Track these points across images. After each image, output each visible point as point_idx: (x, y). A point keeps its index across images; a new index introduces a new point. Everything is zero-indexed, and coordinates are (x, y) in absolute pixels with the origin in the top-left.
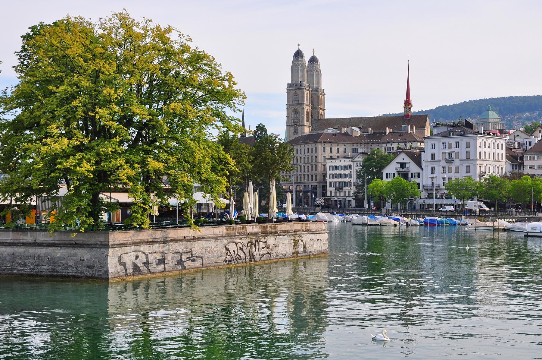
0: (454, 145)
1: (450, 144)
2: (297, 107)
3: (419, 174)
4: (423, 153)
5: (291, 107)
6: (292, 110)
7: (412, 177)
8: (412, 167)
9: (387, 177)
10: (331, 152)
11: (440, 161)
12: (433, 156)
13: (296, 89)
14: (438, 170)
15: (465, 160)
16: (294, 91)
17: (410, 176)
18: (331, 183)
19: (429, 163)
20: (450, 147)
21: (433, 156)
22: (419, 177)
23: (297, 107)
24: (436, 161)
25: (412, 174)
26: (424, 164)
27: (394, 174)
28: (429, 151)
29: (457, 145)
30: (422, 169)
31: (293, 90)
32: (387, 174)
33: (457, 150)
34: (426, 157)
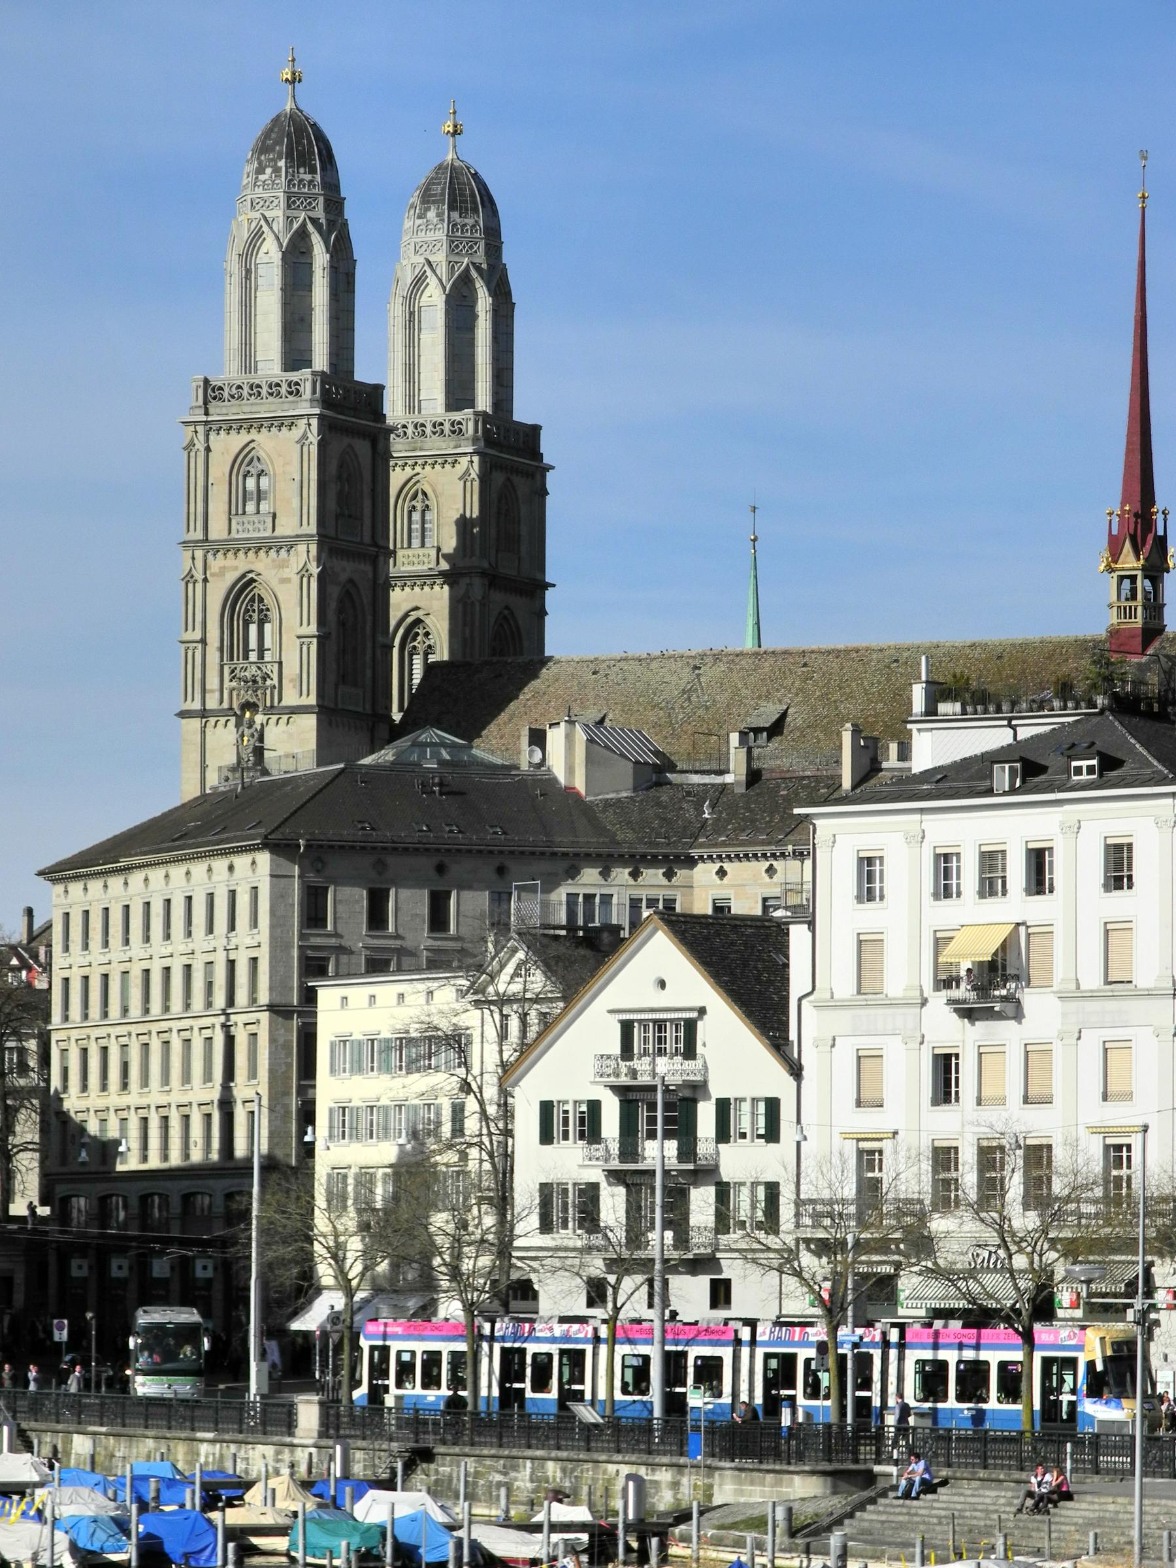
0: (1016, 871)
1: (991, 863)
2: (263, 565)
3: (773, 1106)
4: (798, 935)
5: (216, 564)
6: (217, 592)
7: (723, 1134)
8: (732, 1055)
9: (546, 1137)
10: (377, 919)
11: (924, 1002)
12: (867, 948)
13: (258, 424)
14: (906, 1077)
15: (1092, 996)
16: (237, 441)
17: (706, 1115)
18: (338, 1177)
19: (839, 1021)
20: (991, 883)
21: (867, 948)
22: (772, 1134)
23: (263, 565)
24: (892, 1004)
25: (723, 1107)
26: (809, 1025)
27: (595, 1107)
28: (840, 913)
29: (1039, 874)
30: (796, 1071)
31: (231, 426)
32: (547, 1109)
33: (1036, 909)
34: (816, 965)
